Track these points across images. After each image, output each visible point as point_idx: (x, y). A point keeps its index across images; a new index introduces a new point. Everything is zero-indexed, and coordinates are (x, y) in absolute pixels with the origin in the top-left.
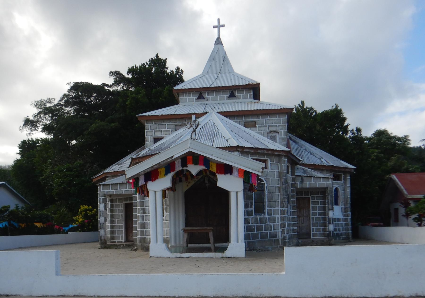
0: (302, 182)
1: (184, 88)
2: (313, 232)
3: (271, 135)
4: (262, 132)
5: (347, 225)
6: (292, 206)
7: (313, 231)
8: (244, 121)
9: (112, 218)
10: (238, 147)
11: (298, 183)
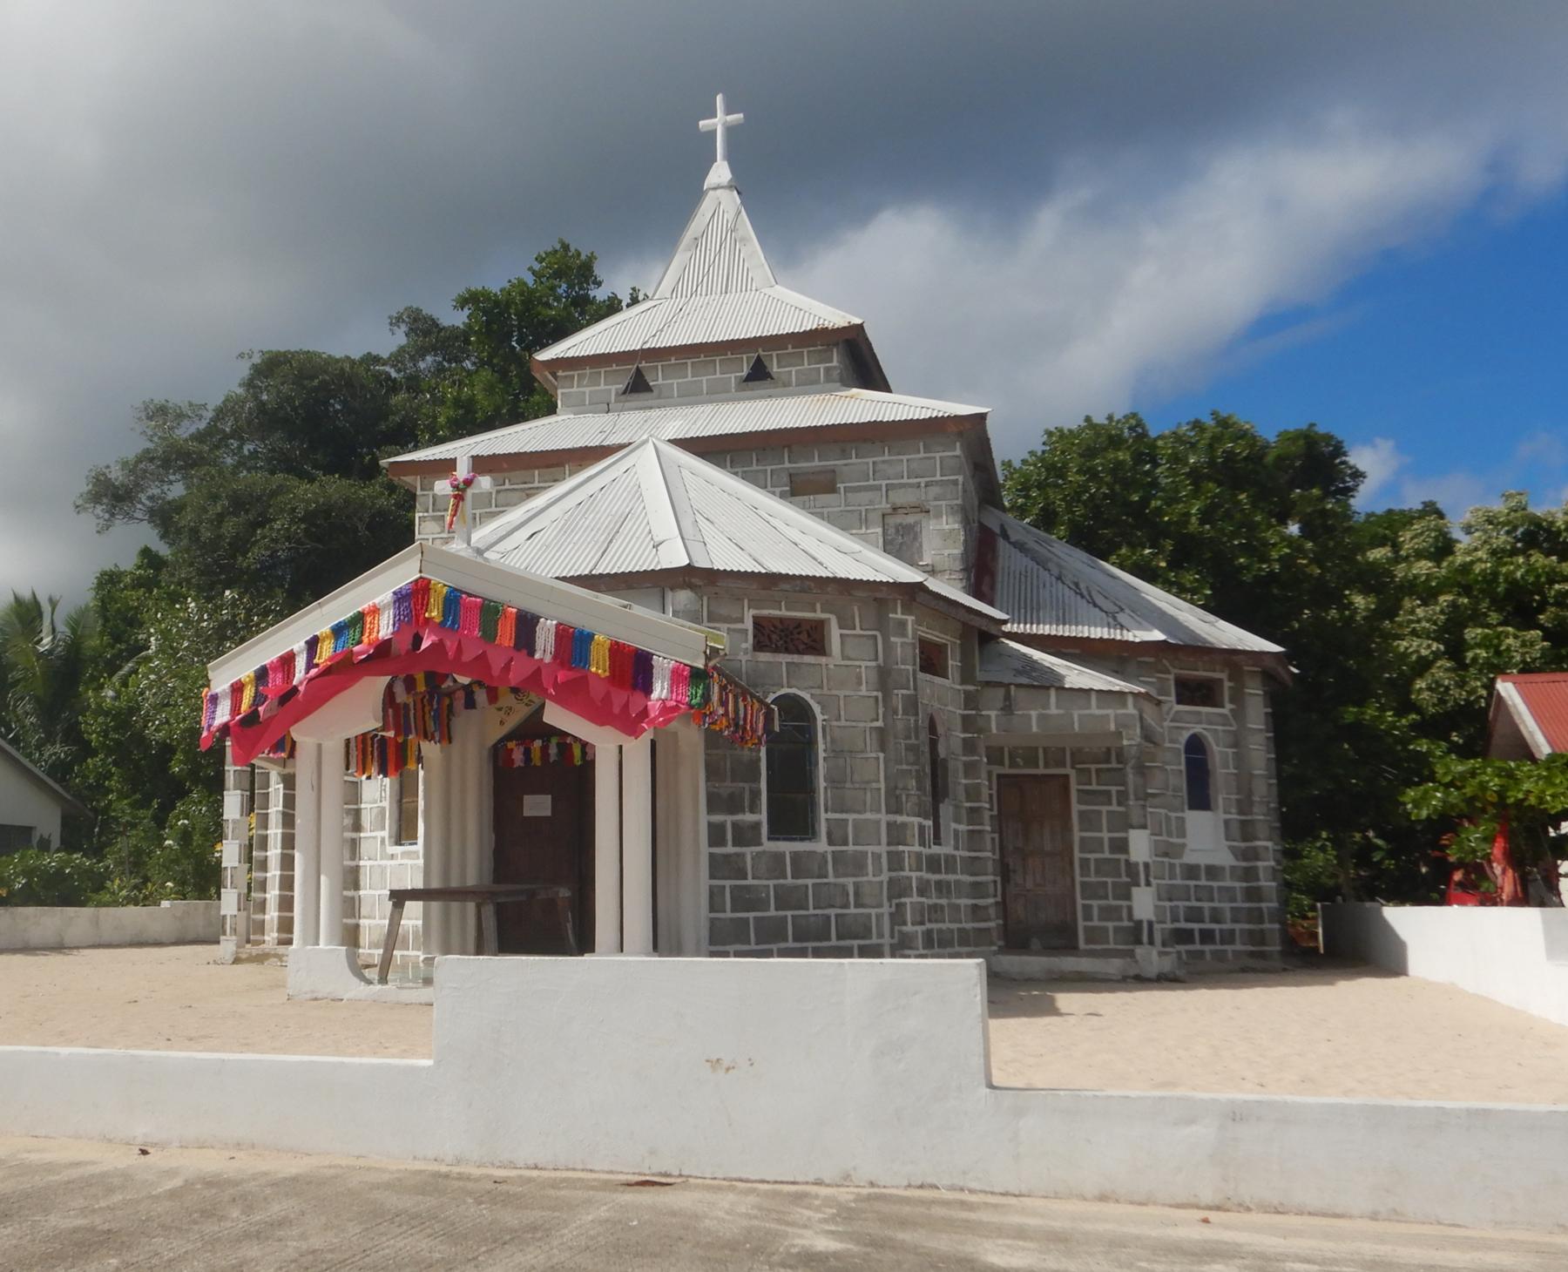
0: (1008, 708)
1: (570, 354)
2: (1089, 924)
3: (899, 519)
4: (861, 511)
5: (1253, 894)
6: (966, 808)
7: (1088, 917)
8: (788, 469)
9: (288, 849)
10: (690, 569)
11: (993, 714)
